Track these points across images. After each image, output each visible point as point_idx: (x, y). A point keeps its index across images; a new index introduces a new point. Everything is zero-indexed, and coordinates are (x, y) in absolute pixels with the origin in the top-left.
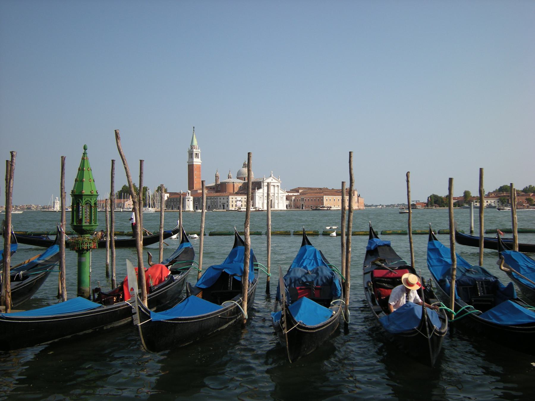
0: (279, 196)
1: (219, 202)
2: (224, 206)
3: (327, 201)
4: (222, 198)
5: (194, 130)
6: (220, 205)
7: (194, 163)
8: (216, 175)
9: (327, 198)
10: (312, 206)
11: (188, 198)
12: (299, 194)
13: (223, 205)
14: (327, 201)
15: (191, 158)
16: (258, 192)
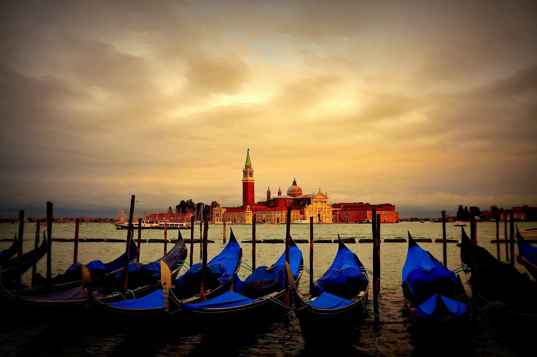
0: (326, 211)
1: (273, 216)
2: (278, 220)
3: (370, 215)
4: (276, 213)
5: (248, 152)
6: (275, 219)
7: (248, 181)
8: (267, 191)
9: (370, 213)
10: (356, 220)
11: (248, 213)
12: (341, 209)
13: (277, 219)
14: (370, 215)
15: (246, 177)
16: (308, 207)
